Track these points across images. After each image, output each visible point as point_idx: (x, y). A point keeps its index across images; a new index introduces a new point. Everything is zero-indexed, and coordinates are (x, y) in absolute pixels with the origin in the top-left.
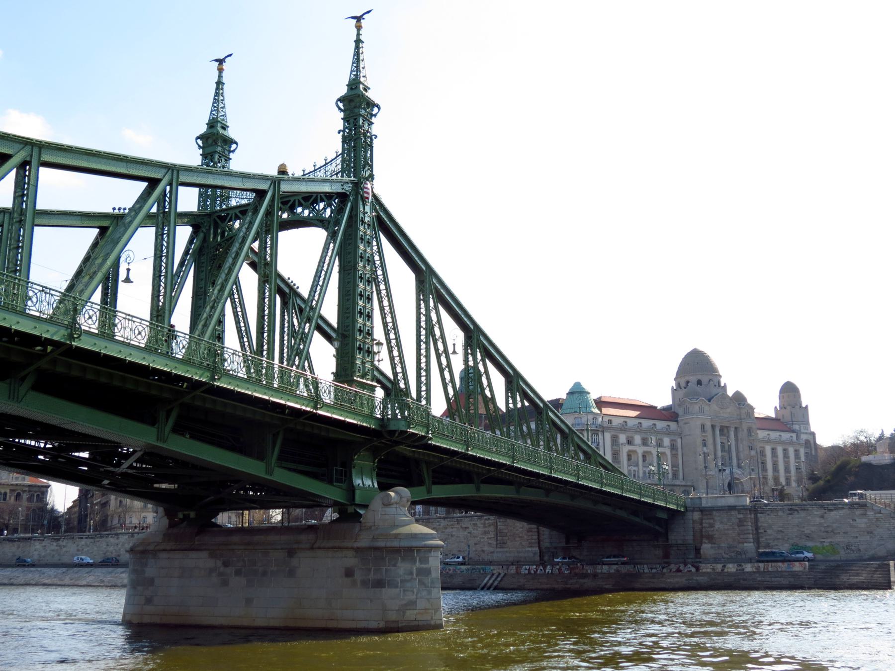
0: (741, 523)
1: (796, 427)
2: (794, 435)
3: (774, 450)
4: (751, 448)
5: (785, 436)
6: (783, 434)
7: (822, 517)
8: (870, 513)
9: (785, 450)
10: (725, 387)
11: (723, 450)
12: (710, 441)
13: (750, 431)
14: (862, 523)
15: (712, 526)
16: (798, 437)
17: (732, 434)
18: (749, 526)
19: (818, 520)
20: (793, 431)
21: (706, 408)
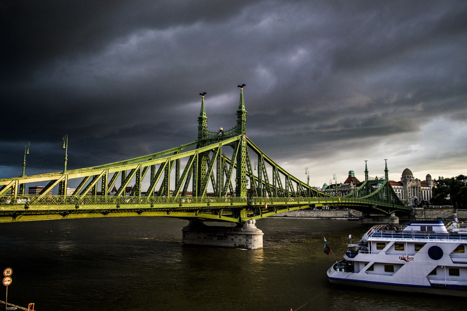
0: (422, 212)
1: (430, 186)
2: (429, 188)
3: (425, 192)
4: (419, 191)
5: (427, 188)
6: (427, 187)
7: (436, 211)
8: (444, 211)
9: (427, 192)
10: (414, 177)
11: (413, 192)
12: (410, 191)
13: (419, 187)
14: (442, 213)
15: (417, 212)
16: (430, 188)
17: (415, 188)
18: (424, 213)
19: (435, 212)
20: (429, 187)
21: (410, 183)
